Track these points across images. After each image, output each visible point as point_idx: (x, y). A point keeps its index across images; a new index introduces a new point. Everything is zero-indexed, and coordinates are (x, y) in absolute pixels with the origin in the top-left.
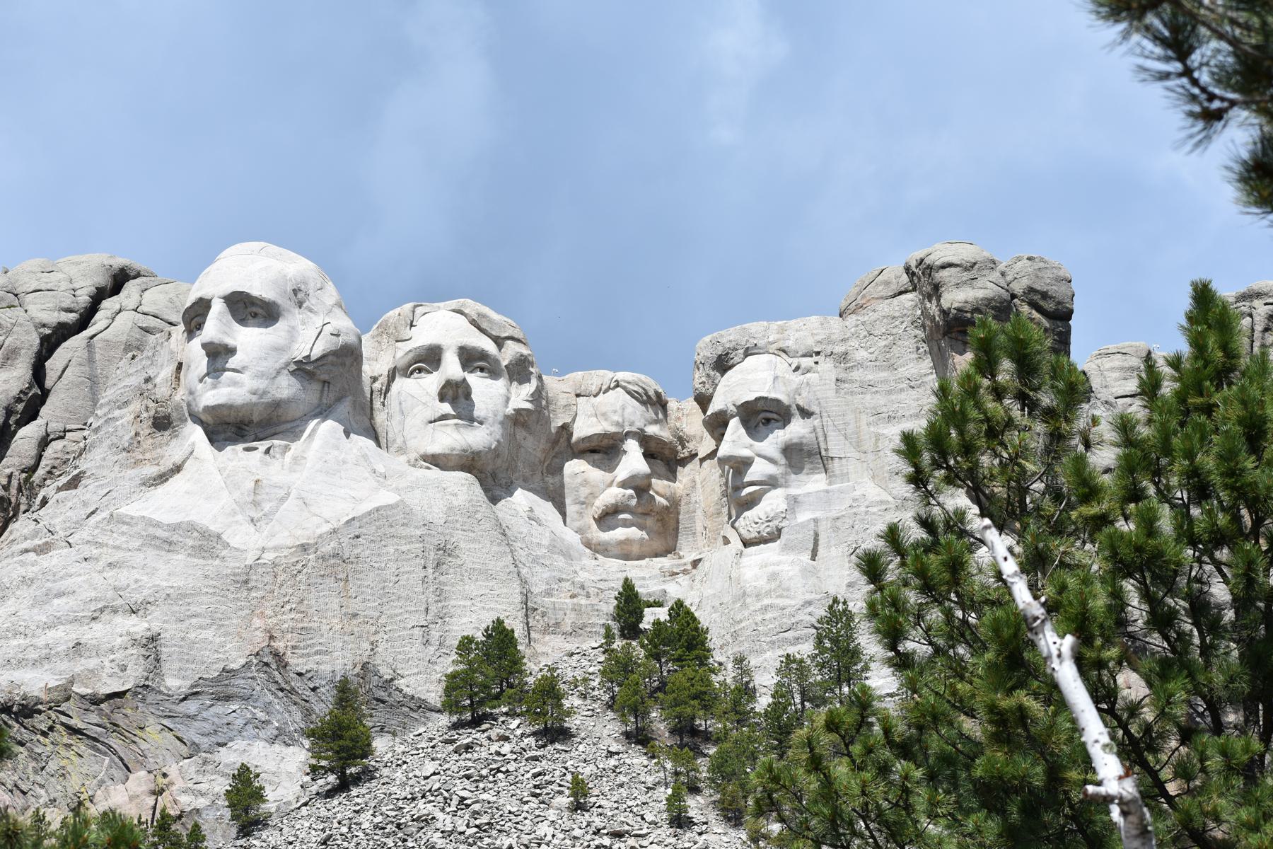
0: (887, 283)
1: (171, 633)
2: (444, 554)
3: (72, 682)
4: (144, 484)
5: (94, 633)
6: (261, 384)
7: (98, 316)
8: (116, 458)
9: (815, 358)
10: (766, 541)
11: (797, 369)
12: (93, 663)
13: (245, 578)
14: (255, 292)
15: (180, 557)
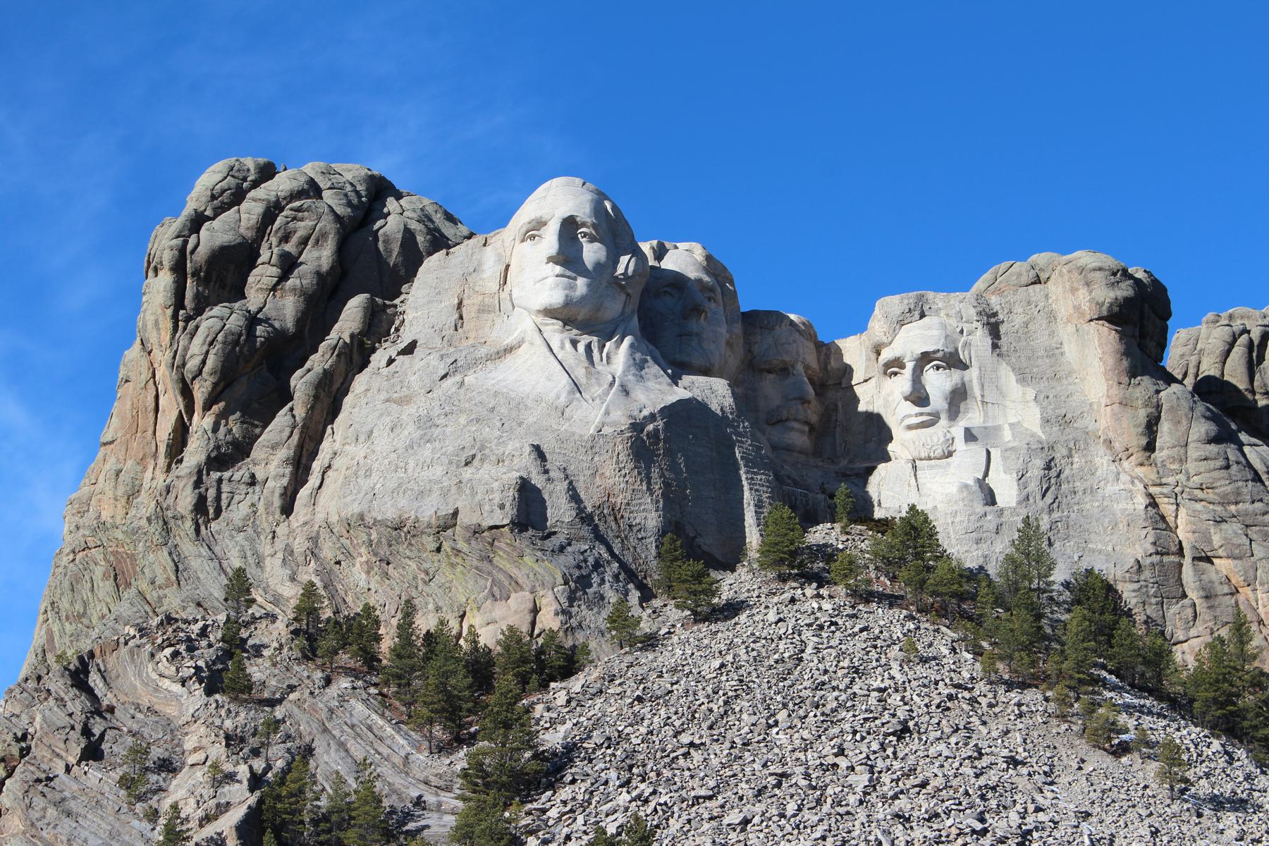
0: (1019, 275)
3: (456, 513)
8: (444, 333)
9: (975, 324)
13: (590, 444)
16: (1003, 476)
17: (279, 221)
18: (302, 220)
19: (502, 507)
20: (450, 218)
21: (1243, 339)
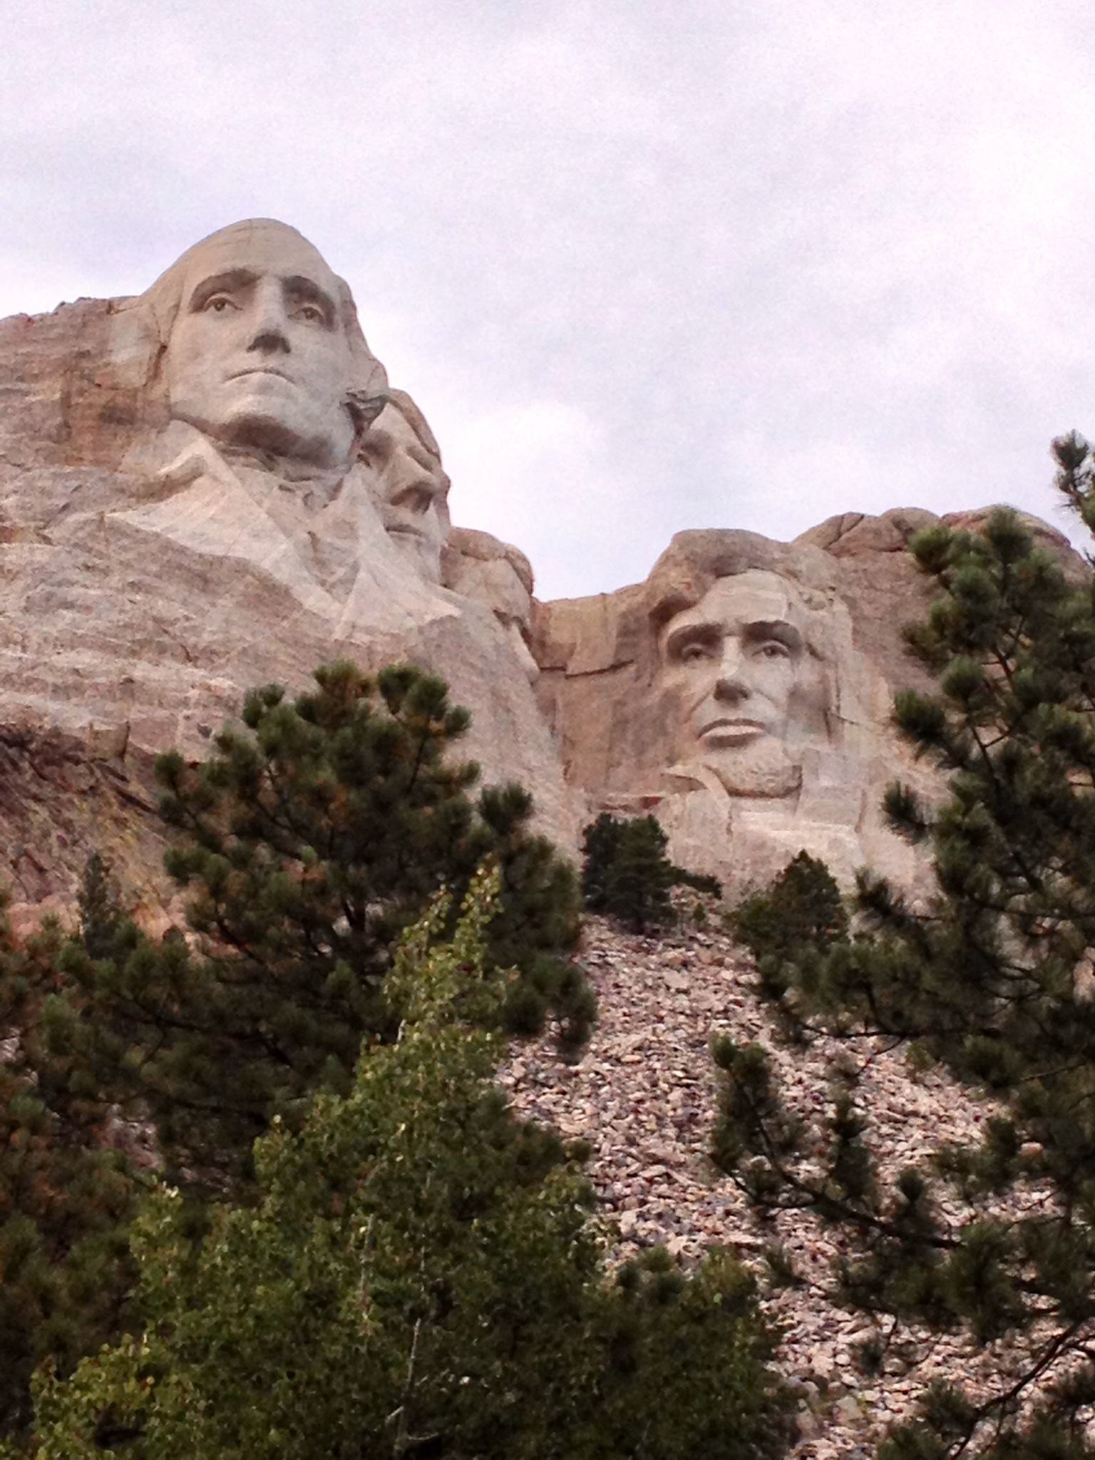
4: (122, 491)
5: (141, 670)
6: (315, 408)
10: (763, 795)
11: (809, 601)
15: (226, 602)
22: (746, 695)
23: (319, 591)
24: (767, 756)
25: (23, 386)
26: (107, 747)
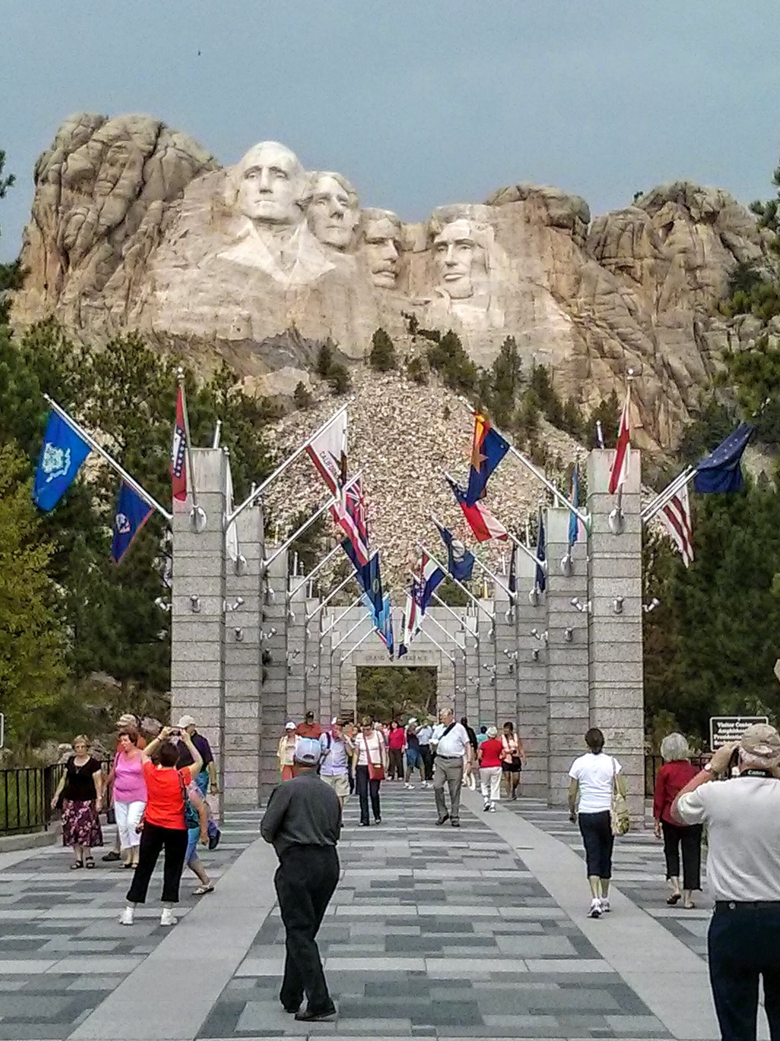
0: (511, 195)
1: (256, 315)
2: (350, 292)
3: (216, 332)
5: (222, 311)
7: (159, 147)
12: (225, 325)
14: (283, 169)
15: (252, 281)
16: (497, 310)
17: (109, 154)
18: (122, 153)
19: (239, 330)
20: (199, 147)
21: (630, 227)
22: (455, 264)
23: (281, 273)
24: (464, 283)
25: (199, 205)
26: (210, 338)
